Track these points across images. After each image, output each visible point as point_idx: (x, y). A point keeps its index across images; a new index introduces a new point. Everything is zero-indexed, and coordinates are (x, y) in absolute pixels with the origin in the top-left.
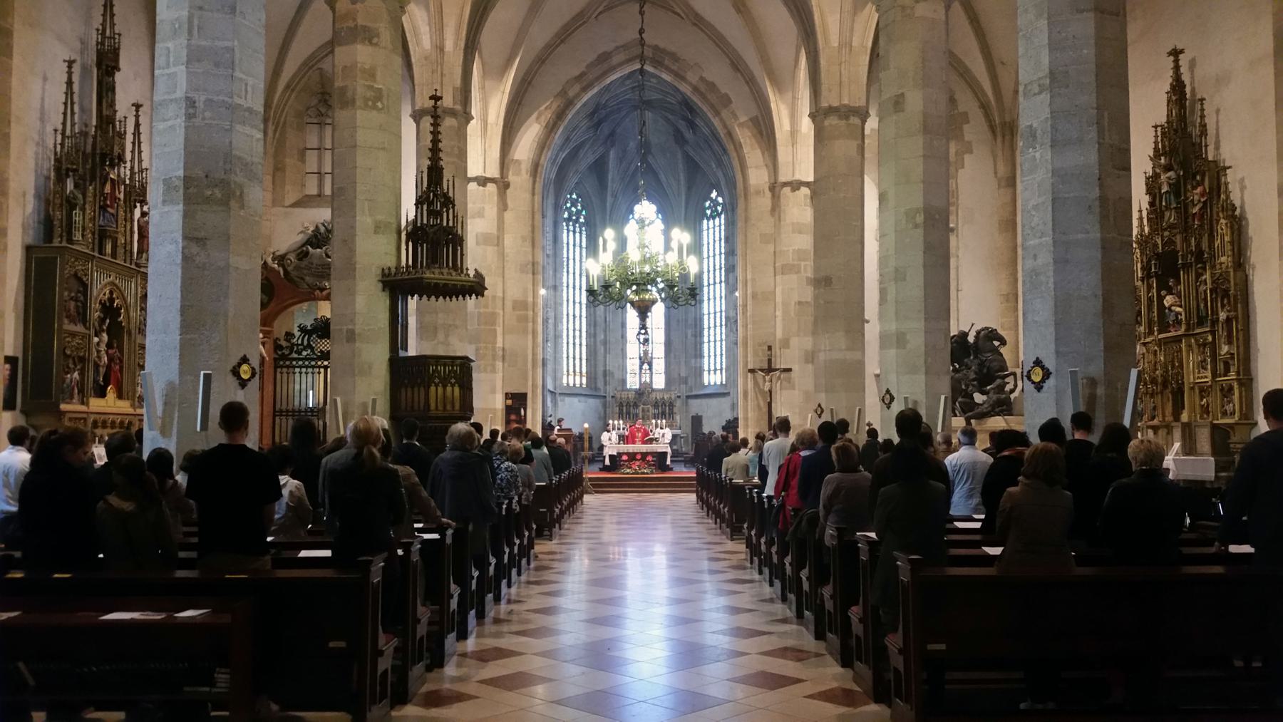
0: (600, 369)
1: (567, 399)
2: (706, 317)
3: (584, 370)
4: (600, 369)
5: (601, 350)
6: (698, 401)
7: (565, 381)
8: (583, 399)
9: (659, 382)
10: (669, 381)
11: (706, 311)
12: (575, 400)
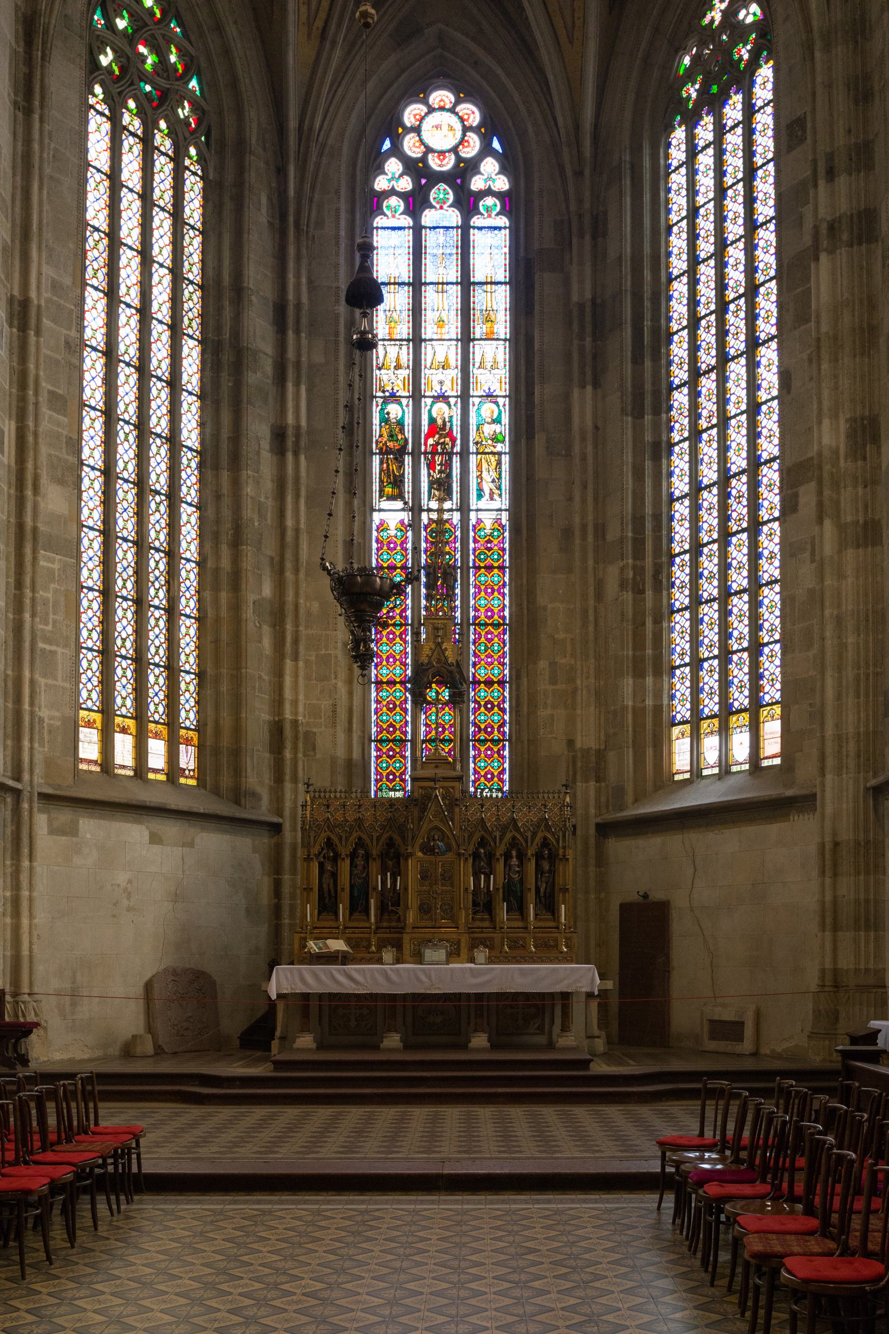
0: (258, 715)
1: (90, 827)
2: (682, 509)
3: (188, 715)
4: (258, 715)
5: (261, 642)
6: (647, 847)
7: (89, 747)
8: (171, 829)
9: (490, 773)
10: (526, 771)
11: (680, 485)
12: (134, 833)
